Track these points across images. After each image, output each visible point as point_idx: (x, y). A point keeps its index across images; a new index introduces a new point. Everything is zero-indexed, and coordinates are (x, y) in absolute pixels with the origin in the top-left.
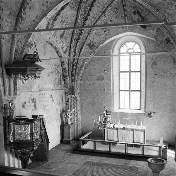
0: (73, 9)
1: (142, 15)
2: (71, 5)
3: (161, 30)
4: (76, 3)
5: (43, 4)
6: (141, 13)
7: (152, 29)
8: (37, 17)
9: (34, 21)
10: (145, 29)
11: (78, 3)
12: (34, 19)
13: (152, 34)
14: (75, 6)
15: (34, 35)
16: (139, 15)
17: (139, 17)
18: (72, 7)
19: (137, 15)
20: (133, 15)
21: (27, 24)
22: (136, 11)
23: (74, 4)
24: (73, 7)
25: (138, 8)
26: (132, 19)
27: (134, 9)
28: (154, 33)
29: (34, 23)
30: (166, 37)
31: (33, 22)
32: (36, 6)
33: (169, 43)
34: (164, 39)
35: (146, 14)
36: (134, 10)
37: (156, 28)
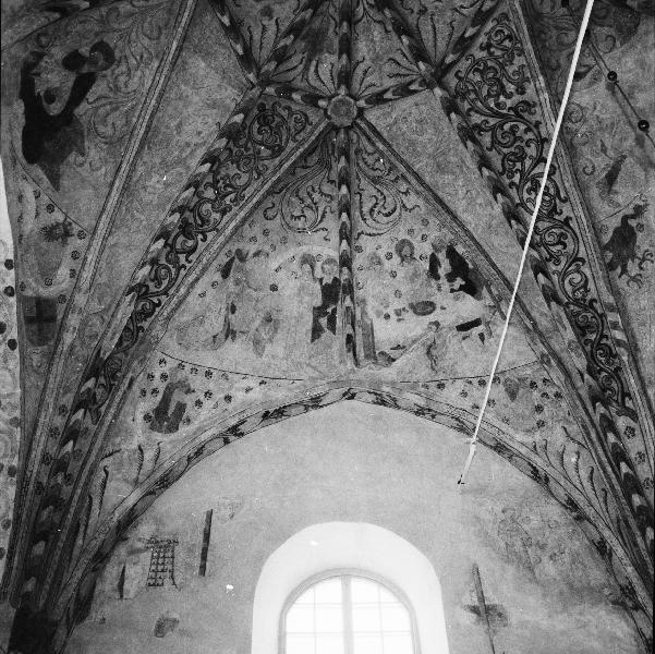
1: (82, 109)
3: (65, 243)
6: (91, 96)
7: (45, 199)
10: (24, 161)
13: (21, 217)
16: (74, 88)
17: (66, 97)
19: (71, 79)
20: (58, 53)
22: (85, 69)
25: (109, 72)
26: (40, 56)
27: (93, 49)
28: (30, 225)
30: (45, 292)
33: (34, 327)
34: (36, 289)
35: (101, 129)
36: (85, 51)
37: (58, 216)
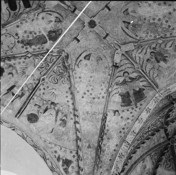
0: (169, 168)
2: (165, 164)
4: (170, 160)
5: (120, 132)
8: (117, 145)
9: (115, 150)
11: (172, 160)
12: (114, 149)
14: (170, 165)
15: (117, 165)
18: (167, 166)
21: (107, 156)
23: (169, 163)
24: (169, 167)
29: (115, 152)
31: (114, 152)
32: (114, 135)
